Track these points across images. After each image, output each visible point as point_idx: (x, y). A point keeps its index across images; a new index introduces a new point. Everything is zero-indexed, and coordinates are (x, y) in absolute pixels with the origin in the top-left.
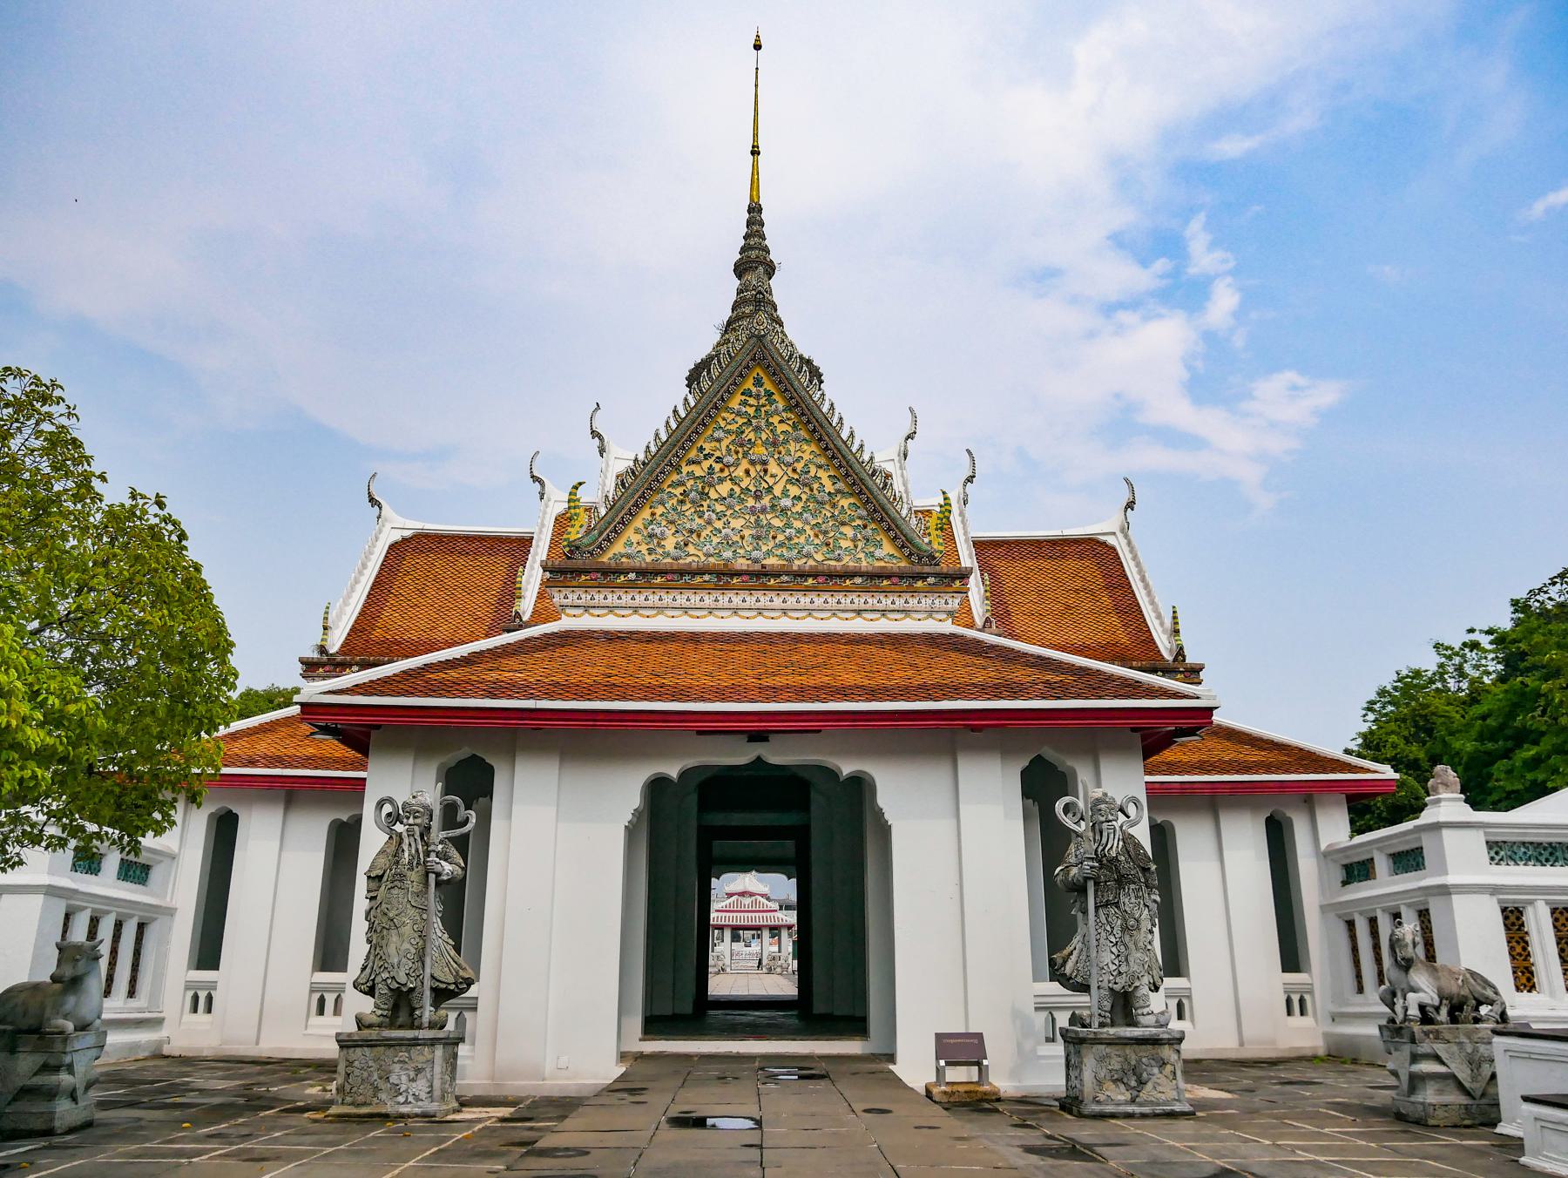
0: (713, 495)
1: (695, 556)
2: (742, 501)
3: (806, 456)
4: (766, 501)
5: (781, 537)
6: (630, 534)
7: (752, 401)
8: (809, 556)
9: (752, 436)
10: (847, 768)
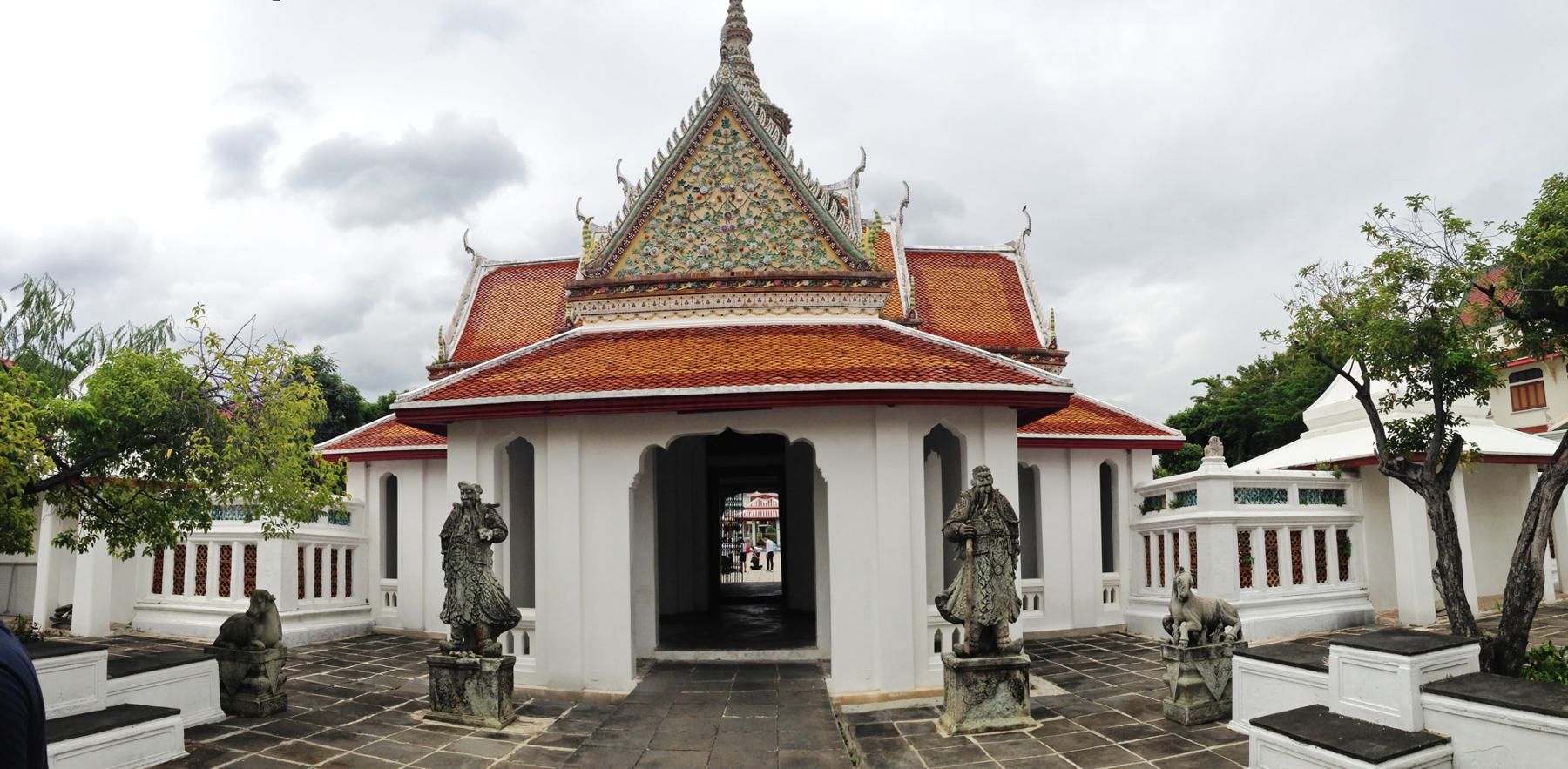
0: (693, 219)
1: (681, 268)
2: (716, 222)
3: (765, 184)
4: (734, 222)
5: (746, 250)
6: (629, 255)
7: (721, 140)
8: (769, 264)
9: (722, 169)
10: (793, 438)
